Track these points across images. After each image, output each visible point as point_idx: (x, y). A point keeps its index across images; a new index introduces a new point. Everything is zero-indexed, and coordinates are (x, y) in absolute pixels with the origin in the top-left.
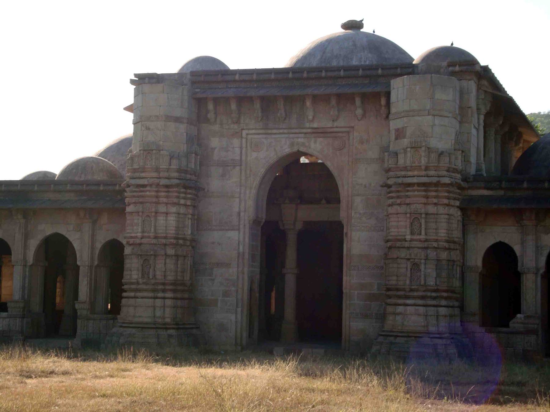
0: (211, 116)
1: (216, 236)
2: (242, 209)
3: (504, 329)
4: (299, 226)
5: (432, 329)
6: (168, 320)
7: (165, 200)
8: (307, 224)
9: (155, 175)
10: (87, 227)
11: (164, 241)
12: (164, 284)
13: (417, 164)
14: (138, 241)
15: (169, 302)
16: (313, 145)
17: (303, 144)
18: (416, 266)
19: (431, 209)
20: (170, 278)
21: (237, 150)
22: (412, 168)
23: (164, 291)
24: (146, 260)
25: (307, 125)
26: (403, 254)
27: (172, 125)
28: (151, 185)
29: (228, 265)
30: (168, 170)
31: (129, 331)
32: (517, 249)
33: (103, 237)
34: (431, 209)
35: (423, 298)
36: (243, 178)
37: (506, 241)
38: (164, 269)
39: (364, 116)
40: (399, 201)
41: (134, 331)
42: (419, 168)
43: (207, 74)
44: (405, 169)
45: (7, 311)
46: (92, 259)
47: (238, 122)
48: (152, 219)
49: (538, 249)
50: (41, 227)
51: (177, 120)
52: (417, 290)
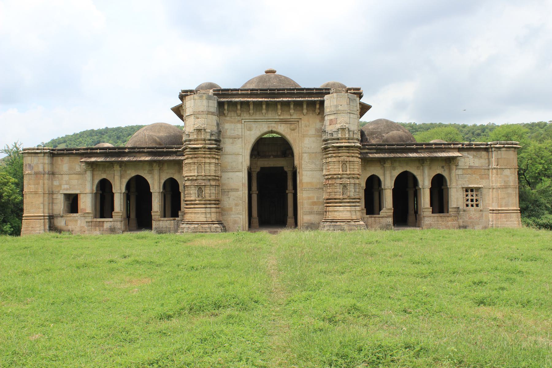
0: (226, 112)
1: (230, 175)
2: (243, 160)
3: (378, 216)
4: (258, 170)
5: (354, 217)
6: (214, 219)
7: (209, 156)
8: (262, 168)
9: (203, 142)
10: (156, 172)
11: (209, 178)
12: (210, 200)
13: (344, 137)
14: (195, 178)
15: (213, 210)
16: (279, 127)
17: (274, 127)
19: (351, 159)
20: (213, 197)
21: (240, 130)
22: (342, 139)
23: (210, 204)
24: (200, 188)
25: (277, 117)
26: (338, 181)
27: (210, 116)
28: (201, 148)
29: (237, 190)
30: (209, 140)
31: (193, 226)
32: (382, 178)
33: (165, 177)
34: (351, 159)
35: (349, 202)
36: (243, 144)
37: (377, 174)
38: (209, 193)
39: (307, 113)
40: (334, 155)
41: (196, 226)
42: (345, 139)
43: (274, 84)
44: (338, 139)
45: (112, 217)
46: (159, 189)
47: (240, 116)
48: (203, 166)
49: (391, 177)
50: (128, 172)
51: (213, 114)
52: (346, 199)
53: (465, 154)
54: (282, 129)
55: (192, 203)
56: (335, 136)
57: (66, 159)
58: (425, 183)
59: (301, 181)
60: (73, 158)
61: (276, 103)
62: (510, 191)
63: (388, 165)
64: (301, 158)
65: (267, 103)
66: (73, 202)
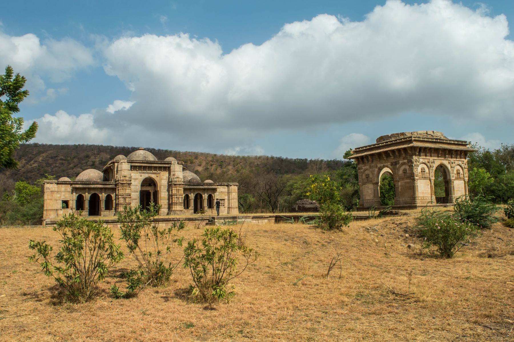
18: (178, 198)
53: (219, 187)
54: (153, 176)
55: (165, 205)
56: (175, 180)
57: (63, 186)
58: (205, 196)
59: (161, 197)
60: (66, 185)
61: (152, 167)
62: (235, 200)
63: (192, 191)
64: (160, 188)
65: (149, 167)
66: (66, 204)
